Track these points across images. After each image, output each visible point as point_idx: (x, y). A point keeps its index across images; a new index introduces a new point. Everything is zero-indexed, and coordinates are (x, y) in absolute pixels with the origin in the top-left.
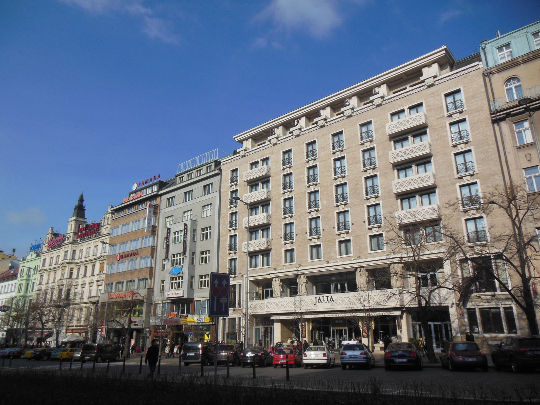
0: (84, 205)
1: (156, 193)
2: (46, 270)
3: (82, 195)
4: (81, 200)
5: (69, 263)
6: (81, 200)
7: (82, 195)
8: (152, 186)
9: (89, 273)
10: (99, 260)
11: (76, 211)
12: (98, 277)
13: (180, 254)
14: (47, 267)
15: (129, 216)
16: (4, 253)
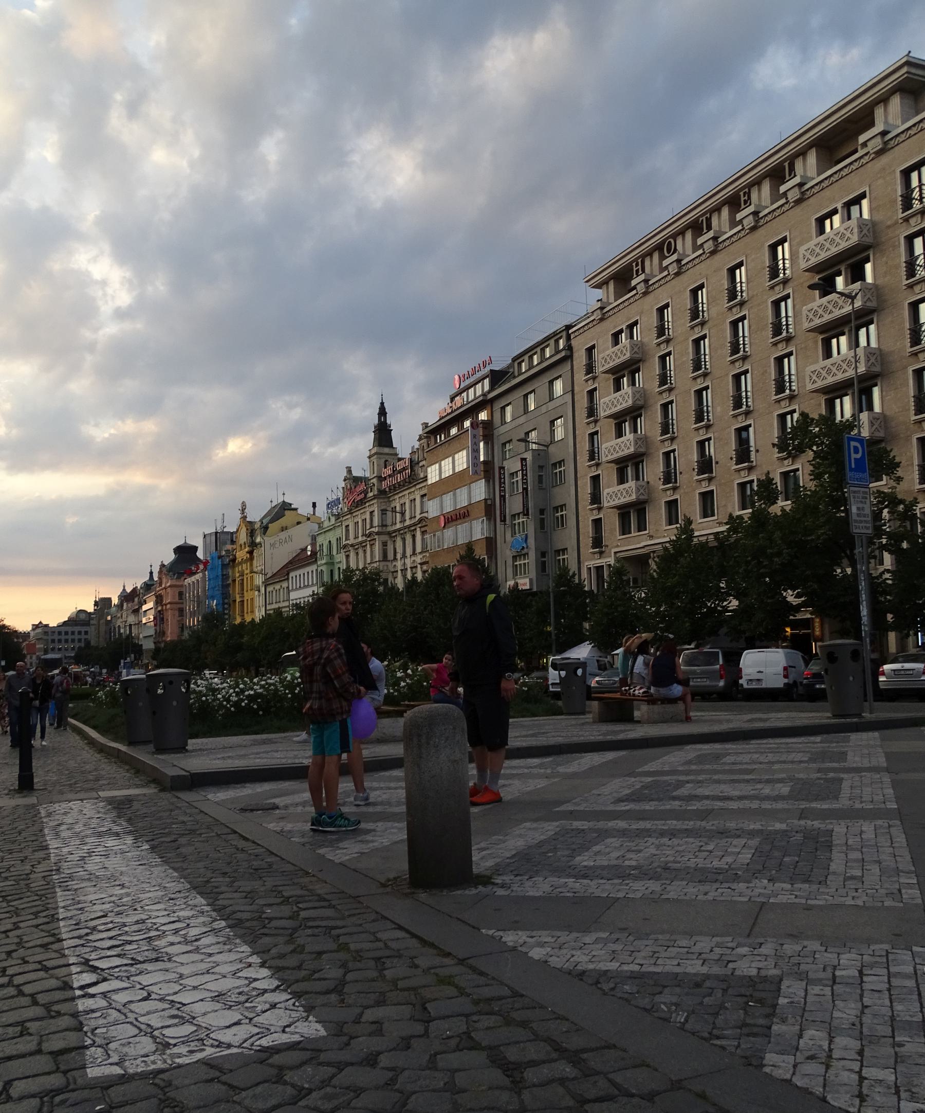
0: (388, 422)
1: (481, 398)
2: (352, 545)
3: (382, 404)
4: (382, 412)
5: (378, 533)
6: (382, 412)
7: (382, 404)
8: (482, 380)
9: (409, 551)
10: (420, 525)
11: (377, 436)
12: (421, 556)
13: (519, 514)
14: (351, 541)
15: (449, 444)
16: (299, 511)
